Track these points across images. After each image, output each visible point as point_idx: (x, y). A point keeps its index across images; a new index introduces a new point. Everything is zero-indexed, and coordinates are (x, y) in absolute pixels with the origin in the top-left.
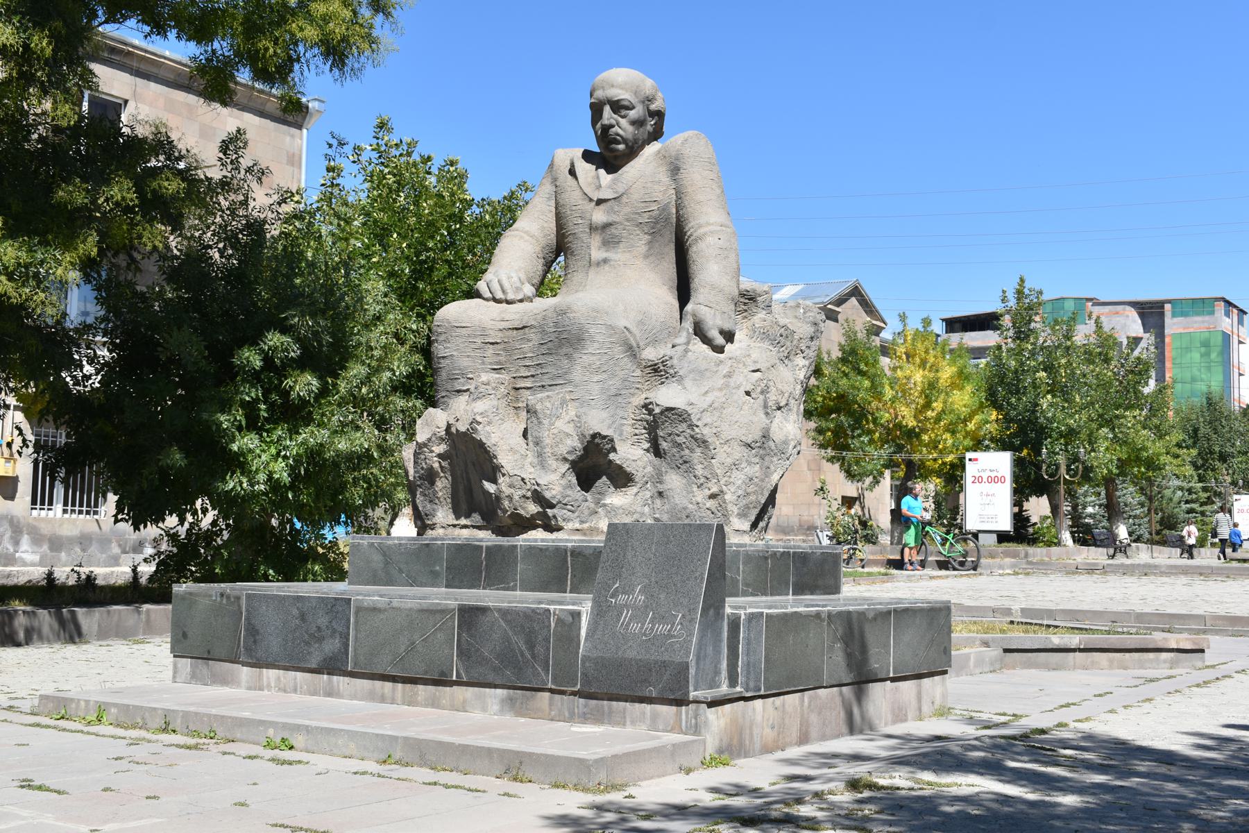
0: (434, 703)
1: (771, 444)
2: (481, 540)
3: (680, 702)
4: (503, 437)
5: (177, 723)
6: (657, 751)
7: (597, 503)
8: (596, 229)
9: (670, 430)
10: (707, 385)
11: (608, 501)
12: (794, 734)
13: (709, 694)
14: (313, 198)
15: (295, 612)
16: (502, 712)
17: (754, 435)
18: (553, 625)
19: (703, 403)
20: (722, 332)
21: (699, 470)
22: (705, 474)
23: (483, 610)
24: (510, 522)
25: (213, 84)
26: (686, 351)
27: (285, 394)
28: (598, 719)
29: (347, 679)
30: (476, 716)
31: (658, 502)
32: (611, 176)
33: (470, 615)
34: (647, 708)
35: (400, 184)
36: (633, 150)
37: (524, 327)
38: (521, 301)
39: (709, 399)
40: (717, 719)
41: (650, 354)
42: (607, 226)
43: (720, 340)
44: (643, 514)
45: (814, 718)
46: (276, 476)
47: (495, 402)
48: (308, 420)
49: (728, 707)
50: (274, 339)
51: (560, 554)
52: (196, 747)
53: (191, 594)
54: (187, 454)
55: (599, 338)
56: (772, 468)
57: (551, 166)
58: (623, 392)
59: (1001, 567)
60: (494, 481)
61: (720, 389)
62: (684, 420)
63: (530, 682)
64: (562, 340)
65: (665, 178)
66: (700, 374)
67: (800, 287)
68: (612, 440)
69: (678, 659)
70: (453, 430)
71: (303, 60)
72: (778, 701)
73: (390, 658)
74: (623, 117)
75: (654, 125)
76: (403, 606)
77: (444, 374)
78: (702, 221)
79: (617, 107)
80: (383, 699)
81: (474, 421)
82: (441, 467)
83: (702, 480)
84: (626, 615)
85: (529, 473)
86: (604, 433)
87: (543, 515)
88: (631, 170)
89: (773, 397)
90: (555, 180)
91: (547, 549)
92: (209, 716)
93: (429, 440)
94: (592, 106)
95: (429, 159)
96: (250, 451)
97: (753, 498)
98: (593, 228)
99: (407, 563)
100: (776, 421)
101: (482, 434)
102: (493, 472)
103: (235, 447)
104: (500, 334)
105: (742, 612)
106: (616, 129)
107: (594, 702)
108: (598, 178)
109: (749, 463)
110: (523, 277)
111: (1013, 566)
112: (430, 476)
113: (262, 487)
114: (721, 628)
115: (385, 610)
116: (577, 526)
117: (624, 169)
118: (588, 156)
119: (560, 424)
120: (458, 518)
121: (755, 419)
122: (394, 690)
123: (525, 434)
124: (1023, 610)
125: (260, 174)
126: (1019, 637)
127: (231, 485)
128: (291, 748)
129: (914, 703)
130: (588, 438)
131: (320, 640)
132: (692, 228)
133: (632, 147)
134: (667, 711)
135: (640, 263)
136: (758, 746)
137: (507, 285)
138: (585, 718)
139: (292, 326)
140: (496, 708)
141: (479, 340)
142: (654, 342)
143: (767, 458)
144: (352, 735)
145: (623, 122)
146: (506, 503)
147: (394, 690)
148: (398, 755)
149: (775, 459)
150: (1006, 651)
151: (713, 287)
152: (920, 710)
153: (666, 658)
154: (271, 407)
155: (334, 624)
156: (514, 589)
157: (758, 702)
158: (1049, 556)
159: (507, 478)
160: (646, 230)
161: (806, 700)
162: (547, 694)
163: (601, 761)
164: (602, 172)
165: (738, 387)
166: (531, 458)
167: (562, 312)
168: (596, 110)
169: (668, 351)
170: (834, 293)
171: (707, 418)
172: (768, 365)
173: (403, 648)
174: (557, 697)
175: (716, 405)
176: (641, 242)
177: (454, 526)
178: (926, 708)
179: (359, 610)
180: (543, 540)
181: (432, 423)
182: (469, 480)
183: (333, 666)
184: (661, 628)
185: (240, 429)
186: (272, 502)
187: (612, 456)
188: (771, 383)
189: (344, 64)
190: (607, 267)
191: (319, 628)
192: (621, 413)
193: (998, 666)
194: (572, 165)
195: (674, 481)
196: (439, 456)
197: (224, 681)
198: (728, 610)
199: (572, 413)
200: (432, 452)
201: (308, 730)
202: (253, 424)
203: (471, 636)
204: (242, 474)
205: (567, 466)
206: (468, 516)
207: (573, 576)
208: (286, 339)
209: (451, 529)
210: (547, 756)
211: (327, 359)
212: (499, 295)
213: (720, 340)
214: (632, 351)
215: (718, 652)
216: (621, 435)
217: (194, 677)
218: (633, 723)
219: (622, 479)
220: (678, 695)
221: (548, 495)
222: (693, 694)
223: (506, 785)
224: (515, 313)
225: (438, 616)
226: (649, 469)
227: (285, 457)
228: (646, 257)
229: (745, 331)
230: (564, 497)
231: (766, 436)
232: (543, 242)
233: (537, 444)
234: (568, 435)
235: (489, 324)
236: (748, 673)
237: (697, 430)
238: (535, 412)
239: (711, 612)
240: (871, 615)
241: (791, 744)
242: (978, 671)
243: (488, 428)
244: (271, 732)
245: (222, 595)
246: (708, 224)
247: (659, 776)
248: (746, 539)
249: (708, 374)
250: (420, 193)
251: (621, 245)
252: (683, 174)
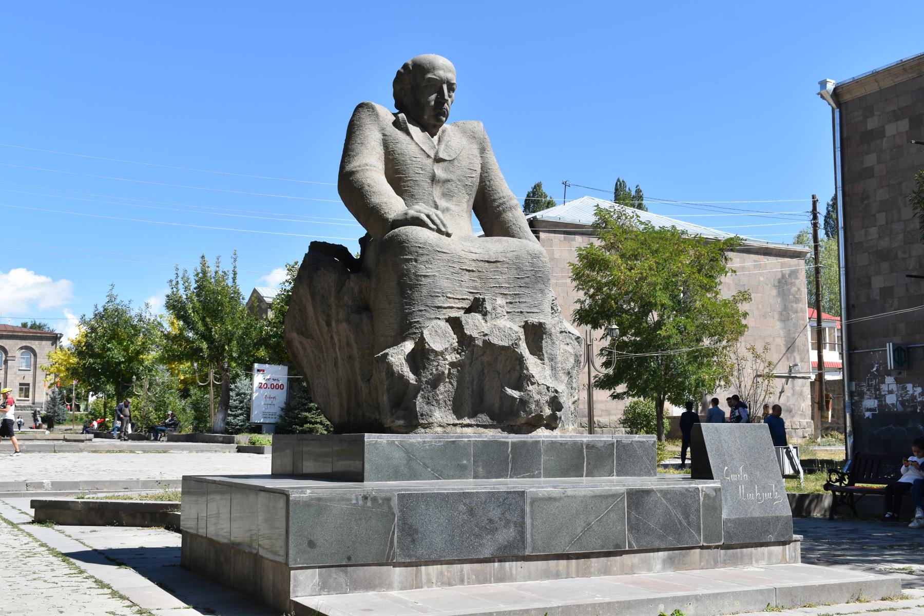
0: (606, 571)
15: (462, 508)
16: (664, 569)
18: (702, 499)
23: (648, 492)
30: (643, 575)
33: (637, 497)
34: (765, 550)
37: (497, 262)
53: (319, 499)
63: (687, 543)
73: (567, 539)
76: (577, 493)
77: (424, 291)
80: (557, 576)
82: (449, 373)
84: (742, 489)
85: (552, 384)
91: (566, 443)
93: (446, 349)
98: (433, 179)
99: (432, 459)
104: (474, 264)
107: (731, 551)
115: (561, 498)
124: (53, 483)
131: (493, 531)
134: (777, 549)
138: (725, 563)
140: (659, 566)
144: (736, 595)
155: (507, 515)
156: (538, 476)
162: (698, 550)
166: (548, 372)
173: (579, 530)
174: (705, 551)
179: (534, 501)
180: (547, 437)
191: (490, 521)
196: (452, 365)
200: (445, 359)
201: (697, 598)
203: (639, 513)
206: (472, 415)
207: (588, 463)
218: (757, 561)
225: (610, 500)
233: (551, 360)
235: (463, 254)
251: (454, 199)
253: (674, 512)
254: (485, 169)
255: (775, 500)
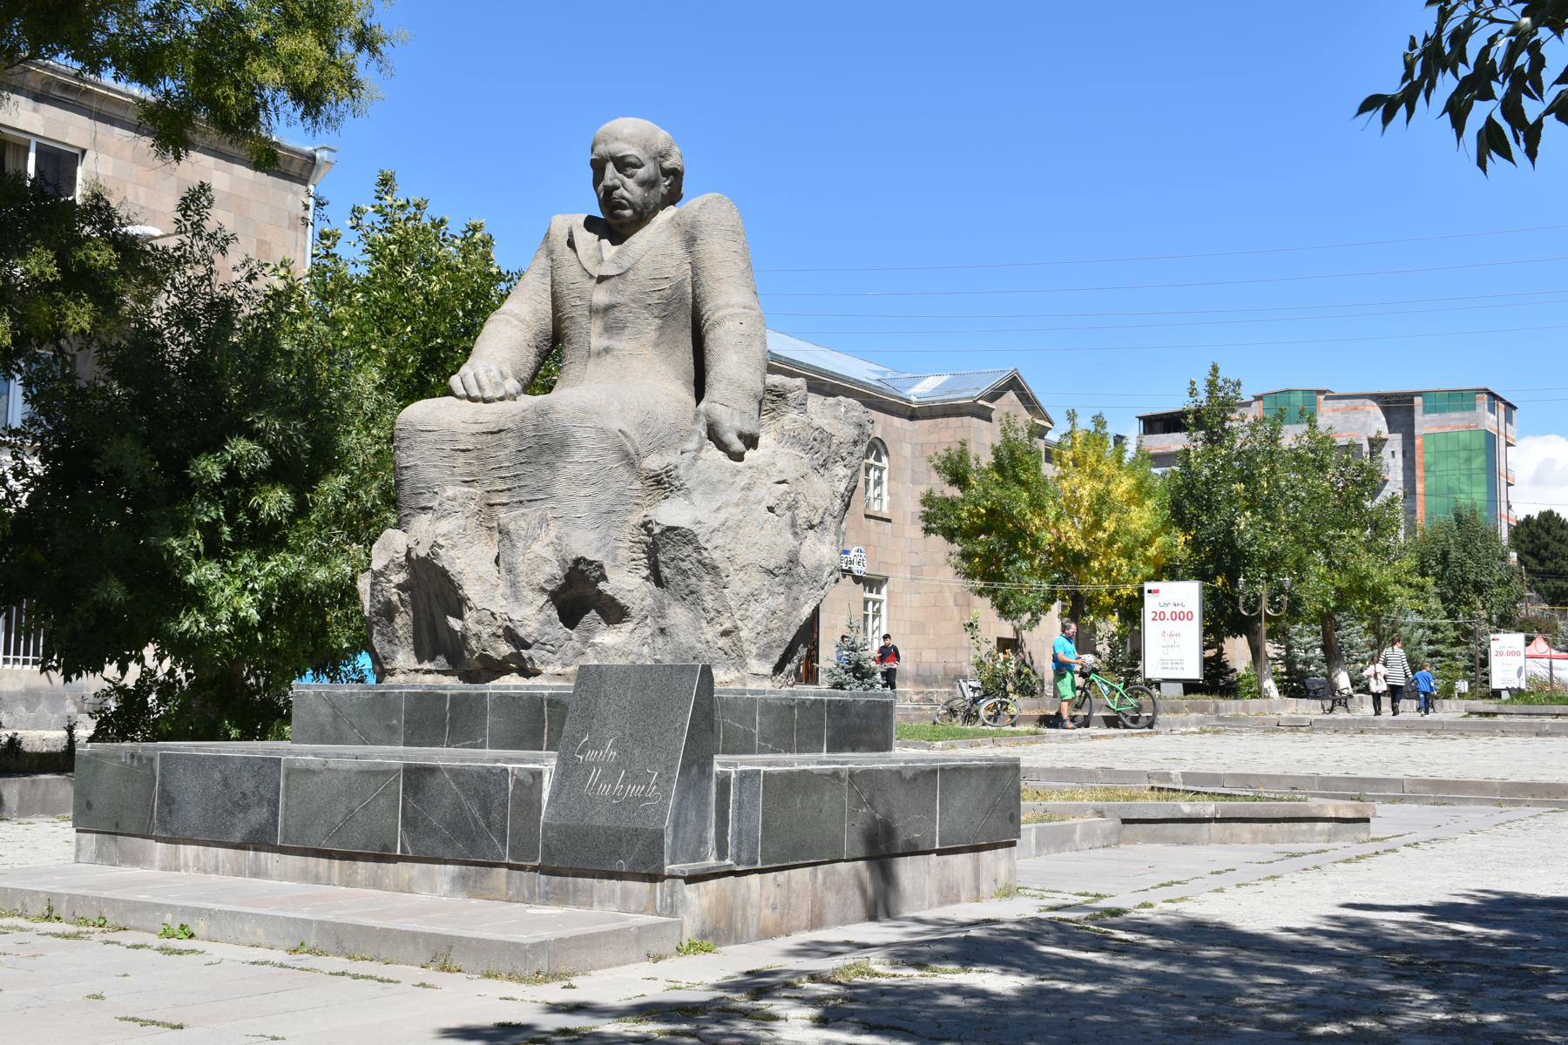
0: (376, 883)
1: (801, 570)
2: (445, 688)
3: (654, 877)
4: (471, 565)
5: (62, 909)
6: (616, 934)
7: (585, 642)
8: (597, 311)
9: (672, 554)
10: (720, 499)
11: (598, 639)
12: (804, 916)
13: (697, 866)
14: (303, 268)
15: (217, 776)
16: (453, 892)
17: (779, 559)
18: (511, 787)
19: (714, 521)
20: (741, 436)
21: (709, 602)
22: (717, 606)
23: (432, 770)
24: (478, 665)
25: (169, 131)
26: (695, 459)
27: (253, 513)
28: (561, 898)
29: (276, 856)
30: (423, 897)
31: (660, 640)
32: (616, 248)
33: (417, 776)
34: (617, 885)
35: (407, 258)
36: (643, 217)
37: (500, 431)
38: (501, 399)
39: (722, 516)
40: (699, 900)
41: (654, 463)
42: (609, 308)
43: (738, 446)
44: (640, 655)
45: (831, 898)
46: (242, 614)
47: (462, 522)
48: (282, 544)
49: (713, 883)
50: (240, 446)
51: (534, 704)
52: (76, 936)
53: (96, 755)
54: (130, 589)
55: (588, 444)
56: (802, 599)
57: (548, 235)
58: (618, 508)
59: (1184, 724)
60: (460, 617)
61: (737, 505)
62: (690, 542)
63: (484, 856)
64: (544, 447)
65: (678, 250)
66: (712, 486)
67: (944, 379)
68: (601, 567)
69: (651, 826)
70: (413, 555)
71: (270, 106)
72: (782, 876)
73: (325, 829)
74: (629, 177)
75: (670, 186)
78: (720, 302)
79: (622, 164)
80: (317, 880)
81: (436, 544)
82: (401, 600)
83: (713, 614)
84: (595, 774)
85: (500, 606)
86: (590, 558)
87: (517, 657)
88: (640, 241)
89: (802, 514)
90: (551, 252)
91: (520, 697)
92: (98, 899)
93: (386, 567)
94: (594, 163)
95: (442, 221)
96: (210, 583)
97: (776, 635)
98: (593, 311)
100: (807, 543)
101: (446, 560)
102: (457, 605)
103: (191, 579)
104: (473, 440)
105: (733, 770)
106: (621, 191)
107: (557, 879)
108: (600, 249)
109: (772, 593)
110: (507, 369)
111: (1199, 722)
112: (387, 612)
113: (225, 628)
114: (708, 789)
115: (321, 772)
116: (559, 669)
117: (631, 239)
118: (591, 224)
119: (540, 548)
120: (420, 661)
121: (780, 540)
122: (330, 867)
123: (497, 561)
124: (1184, 775)
125: (223, 243)
126: (1152, 806)
127: (186, 625)
128: (192, 936)
129: (969, 881)
130: (570, 564)
131: (246, 809)
132: (711, 312)
133: (641, 213)
135: (649, 352)
136: (753, 930)
137: (484, 380)
138: (547, 898)
139: (259, 430)
140: (446, 887)
141: (447, 447)
142: (661, 447)
143: (795, 588)
144: (260, 919)
145: (630, 182)
146: (473, 643)
147: (330, 867)
148: (311, 943)
149: (806, 588)
150: (1125, 821)
151: (731, 382)
152: (978, 889)
153: (639, 825)
154: (237, 529)
156: (482, 747)
157: (755, 878)
158: (1246, 709)
159: (474, 613)
160: (656, 312)
161: (820, 876)
162: (504, 871)
163: (540, 946)
164: (605, 242)
165: (760, 502)
167: (543, 413)
168: (598, 166)
169: (671, 458)
170: (986, 386)
171: (718, 540)
172: (797, 475)
174: (516, 873)
175: (729, 523)
176: (649, 327)
177: (417, 671)
178: (985, 888)
180: (516, 687)
181: (391, 545)
182: (432, 615)
183: (260, 840)
184: (634, 790)
185: (197, 556)
186: (239, 647)
187: (601, 586)
188: (801, 497)
189: (318, 112)
190: (609, 358)
191: (244, 795)
192: (615, 534)
193: (1114, 840)
194: (571, 235)
195: (678, 615)
196: (399, 586)
197: (134, 860)
198: (717, 768)
199: (553, 534)
201: (210, 914)
202: (214, 550)
203: (418, 802)
204: (201, 611)
205: (546, 597)
206: (432, 659)
207: (551, 730)
208: (250, 446)
209: (412, 674)
210: (478, 940)
211: (299, 469)
212: (475, 392)
213: (738, 446)
214: (630, 460)
215: (703, 817)
216: (614, 559)
217: (100, 856)
218: (601, 903)
219: (614, 613)
220: (651, 869)
221: (522, 632)
222: (668, 868)
223: (431, 976)
224: (490, 415)
226: (649, 601)
227: (253, 591)
228: (656, 345)
229: (773, 434)
230: (543, 635)
231: (793, 560)
232: (536, 327)
233: (510, 571)
234: (546, 560)
235: (460, 428)
236: (740, 842)
237: (705, 554)
238: (508, 533)
239: (694, 770)
240: (909, 775)
241: (799, 929)
242: (1086, 846)
243: (451, 553)
244: (168, 918)
245: (133, 756)
246: (728, 305)
247: (618, 965)
248: (767, 685)
249: (722, 486)
250: (428, 265)
251: (627, 331)
252: (701, 246)
253: (467, 804)
254: (696, 269)
255: (648, 799)
